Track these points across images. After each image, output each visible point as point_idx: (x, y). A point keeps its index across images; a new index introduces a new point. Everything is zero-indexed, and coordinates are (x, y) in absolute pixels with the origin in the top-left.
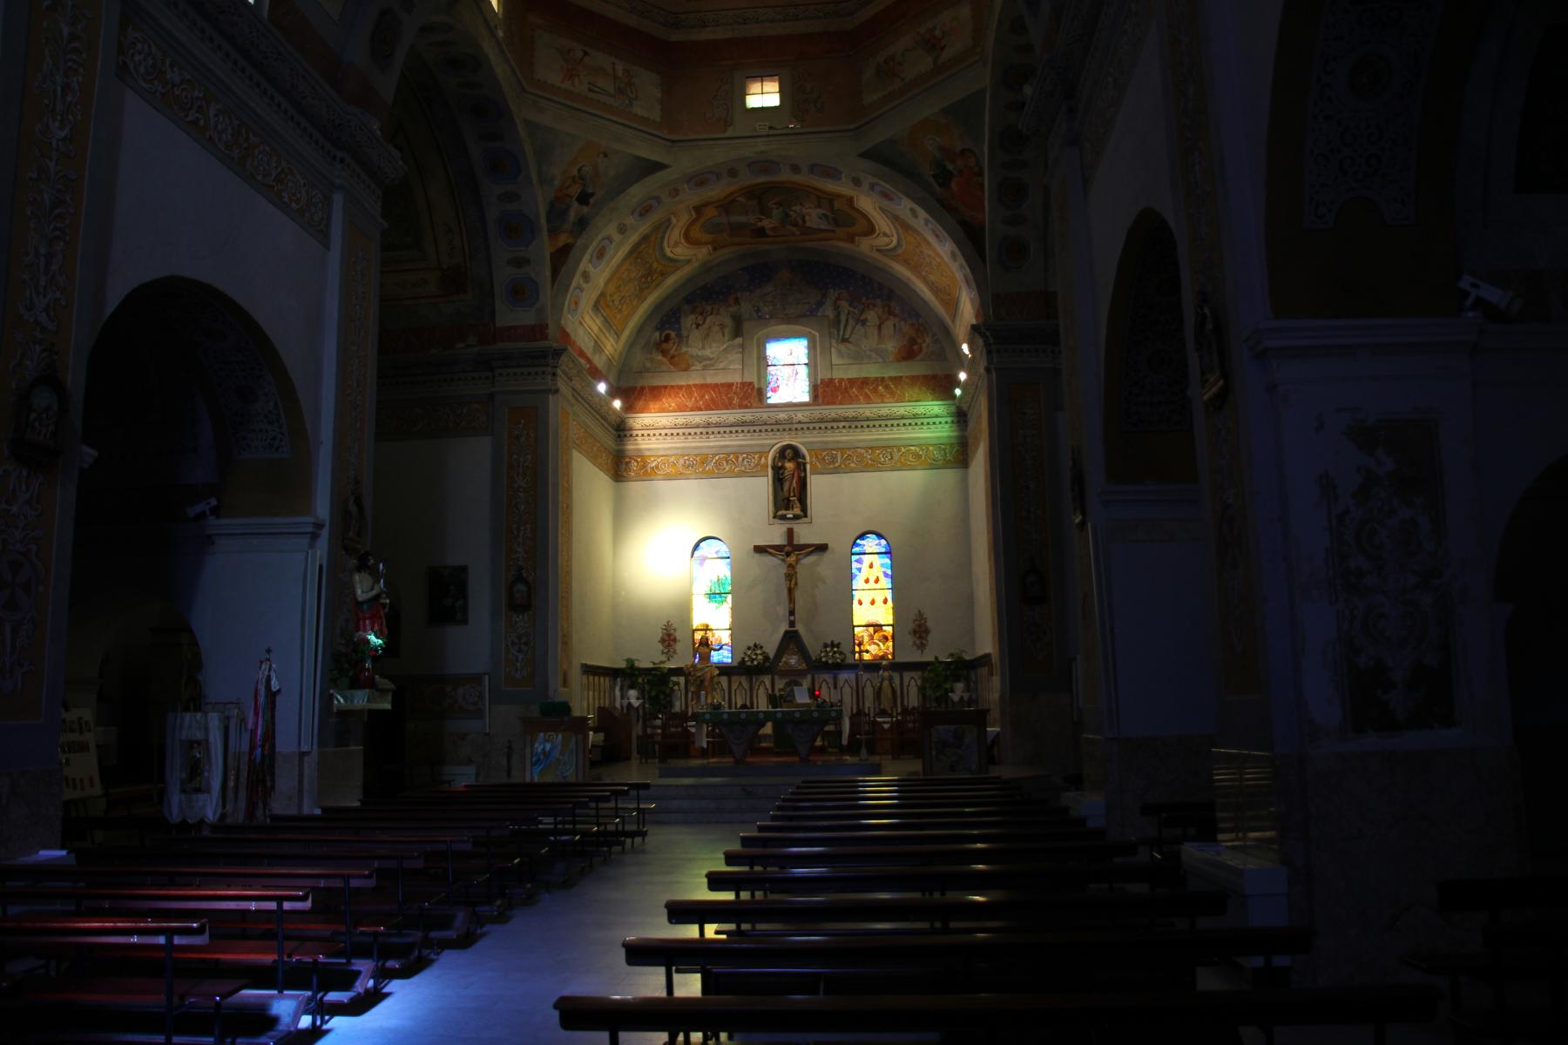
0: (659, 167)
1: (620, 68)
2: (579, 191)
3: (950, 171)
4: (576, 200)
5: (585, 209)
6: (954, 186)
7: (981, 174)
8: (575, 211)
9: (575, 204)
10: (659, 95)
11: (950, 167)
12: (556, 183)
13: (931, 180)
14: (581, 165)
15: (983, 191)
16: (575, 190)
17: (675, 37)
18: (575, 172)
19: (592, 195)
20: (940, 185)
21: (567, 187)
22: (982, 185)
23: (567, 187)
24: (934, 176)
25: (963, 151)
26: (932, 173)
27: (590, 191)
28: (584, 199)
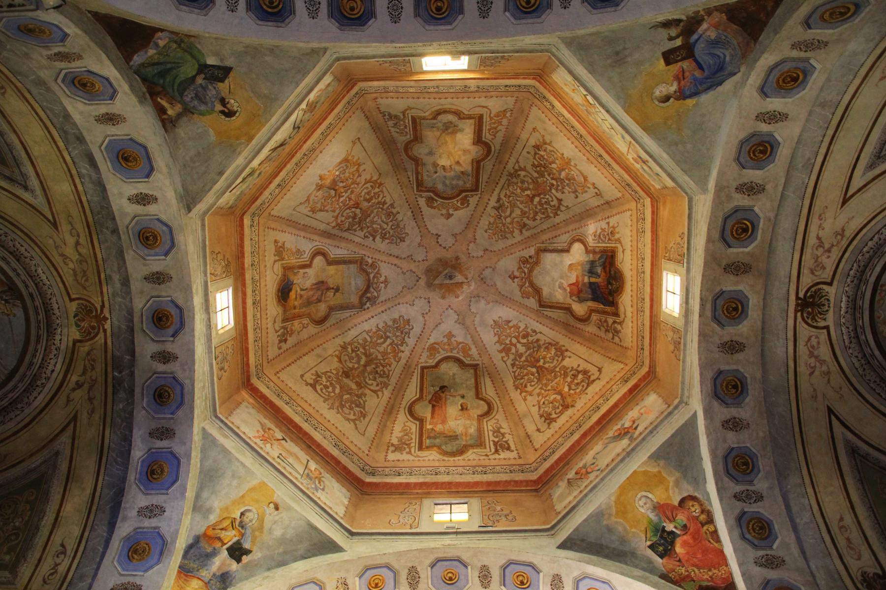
0: (332, 547)
1: (313, 466)
2: (235, 539)
3: (672, 532)
4: (228, 549)
5: (234, 566)
6: (679, 549)
7: (710, 520)
8: (221, 561)
9: (225, 554)
10: (347, 503)
11: (670, 527)
12: (213, 518)
13: (650, 553)
14: (246, 508)
15: (718, 540)
16: (230, 537)
17: (369, 479)
18: (237, 515)
19: (247, 552)
20: (662, 556)
21: (222, 529)
22: (715, 533)
23: (222, 529)
24: (651, 547)
25: (682, 501)
26: (649, 543)
27: (247, 546)
28: (237, 552)
